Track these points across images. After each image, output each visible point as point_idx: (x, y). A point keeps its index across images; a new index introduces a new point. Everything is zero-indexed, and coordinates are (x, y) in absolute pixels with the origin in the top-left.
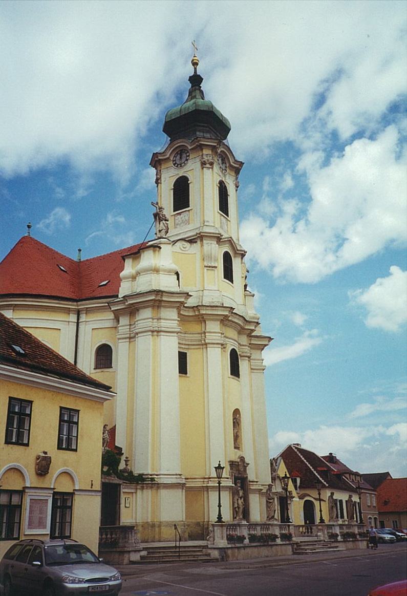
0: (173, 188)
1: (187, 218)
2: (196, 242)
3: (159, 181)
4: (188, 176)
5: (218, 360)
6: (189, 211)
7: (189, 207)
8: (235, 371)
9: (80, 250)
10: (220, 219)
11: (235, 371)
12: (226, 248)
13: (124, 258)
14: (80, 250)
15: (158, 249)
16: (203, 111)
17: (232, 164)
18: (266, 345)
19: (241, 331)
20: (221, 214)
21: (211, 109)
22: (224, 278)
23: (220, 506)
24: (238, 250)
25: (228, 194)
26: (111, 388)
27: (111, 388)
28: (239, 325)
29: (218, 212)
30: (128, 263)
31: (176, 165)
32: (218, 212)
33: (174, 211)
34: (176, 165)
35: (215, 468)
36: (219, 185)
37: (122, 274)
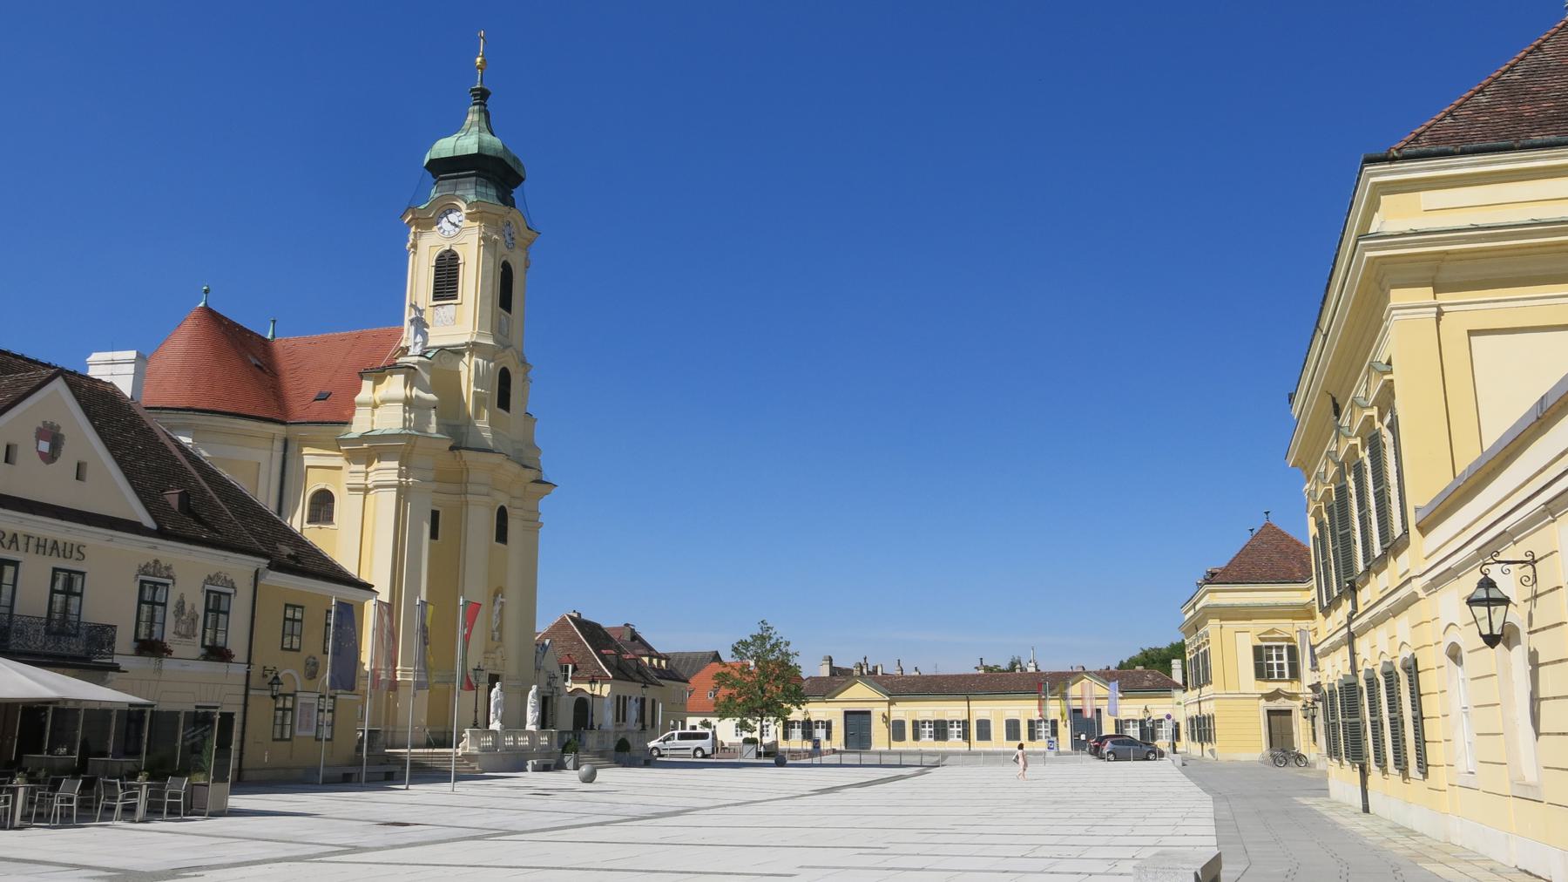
0: (434, 264)
1: (453, 314)
6: (456, 304)
7: (456, 298)
8: (502, 535)
10: (500, 319)
11: (502, 535)
13: (362, 376)
14: (274, 321)
16: (491, 156)
23: (476, 712)
26: (373, 586)
30: (367, 385)
31: (442, 231)
33: (434, 300)
34: (442, 231)
35: (474, 670)
37: (358, 398)
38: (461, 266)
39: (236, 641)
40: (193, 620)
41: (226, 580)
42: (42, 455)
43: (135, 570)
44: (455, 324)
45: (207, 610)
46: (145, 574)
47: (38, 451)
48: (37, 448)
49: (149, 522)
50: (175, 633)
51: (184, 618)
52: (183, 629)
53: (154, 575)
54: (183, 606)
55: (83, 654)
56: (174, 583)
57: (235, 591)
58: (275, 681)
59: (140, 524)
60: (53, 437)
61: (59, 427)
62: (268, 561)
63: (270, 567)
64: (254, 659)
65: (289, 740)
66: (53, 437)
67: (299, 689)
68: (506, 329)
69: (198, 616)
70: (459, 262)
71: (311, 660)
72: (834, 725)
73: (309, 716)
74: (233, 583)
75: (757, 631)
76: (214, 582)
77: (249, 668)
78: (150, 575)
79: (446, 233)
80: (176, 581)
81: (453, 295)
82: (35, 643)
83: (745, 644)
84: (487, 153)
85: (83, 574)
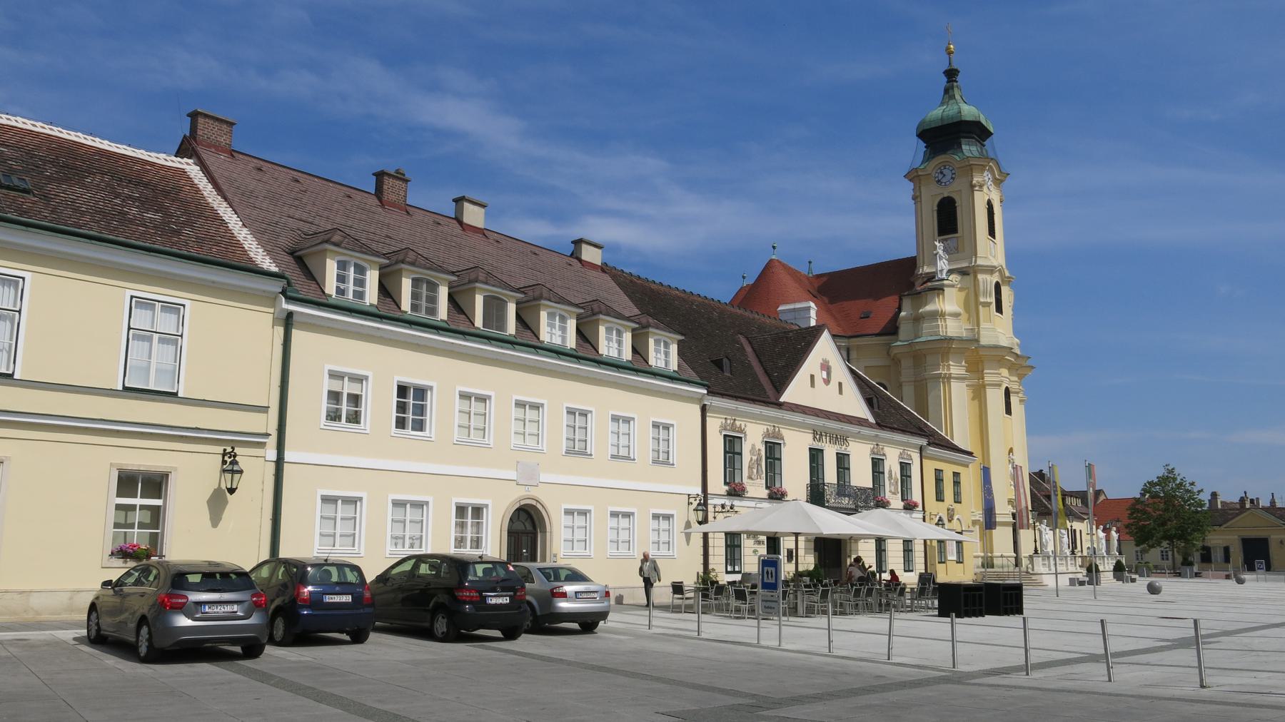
2: (968, 274)
3: (919, 199)
4: (954, 197)
5: (995, 398)
6: (957, 237)
9: (810, 262)
12: (996, 278)
14: (810, 262)
15: (941, 291)
18: (1026, 375)
19: (1012, 368)
21: (978, 120)
23: (1035, 541)
24: (1005, 277)
26: (973, 453)
28: (1011, 361)
39: (916, 496)
43: (869, 452)
44: (958, 252)
45: (902, 476)
46: (874, 453)
49: (872, 420)
51: (892, 481)
52: (893, 488)
55: (853, 507)
58: (940, 523)
60: (826, 367)
63: (929, 444)
64: (926, 509)
65: (944, 563)
66: (826, 367)
72: (1232, 550)
75: (1161, 472)
79: (943, 184)
81: (955, 231)
83: (1151, 484)
85: (849, 455)
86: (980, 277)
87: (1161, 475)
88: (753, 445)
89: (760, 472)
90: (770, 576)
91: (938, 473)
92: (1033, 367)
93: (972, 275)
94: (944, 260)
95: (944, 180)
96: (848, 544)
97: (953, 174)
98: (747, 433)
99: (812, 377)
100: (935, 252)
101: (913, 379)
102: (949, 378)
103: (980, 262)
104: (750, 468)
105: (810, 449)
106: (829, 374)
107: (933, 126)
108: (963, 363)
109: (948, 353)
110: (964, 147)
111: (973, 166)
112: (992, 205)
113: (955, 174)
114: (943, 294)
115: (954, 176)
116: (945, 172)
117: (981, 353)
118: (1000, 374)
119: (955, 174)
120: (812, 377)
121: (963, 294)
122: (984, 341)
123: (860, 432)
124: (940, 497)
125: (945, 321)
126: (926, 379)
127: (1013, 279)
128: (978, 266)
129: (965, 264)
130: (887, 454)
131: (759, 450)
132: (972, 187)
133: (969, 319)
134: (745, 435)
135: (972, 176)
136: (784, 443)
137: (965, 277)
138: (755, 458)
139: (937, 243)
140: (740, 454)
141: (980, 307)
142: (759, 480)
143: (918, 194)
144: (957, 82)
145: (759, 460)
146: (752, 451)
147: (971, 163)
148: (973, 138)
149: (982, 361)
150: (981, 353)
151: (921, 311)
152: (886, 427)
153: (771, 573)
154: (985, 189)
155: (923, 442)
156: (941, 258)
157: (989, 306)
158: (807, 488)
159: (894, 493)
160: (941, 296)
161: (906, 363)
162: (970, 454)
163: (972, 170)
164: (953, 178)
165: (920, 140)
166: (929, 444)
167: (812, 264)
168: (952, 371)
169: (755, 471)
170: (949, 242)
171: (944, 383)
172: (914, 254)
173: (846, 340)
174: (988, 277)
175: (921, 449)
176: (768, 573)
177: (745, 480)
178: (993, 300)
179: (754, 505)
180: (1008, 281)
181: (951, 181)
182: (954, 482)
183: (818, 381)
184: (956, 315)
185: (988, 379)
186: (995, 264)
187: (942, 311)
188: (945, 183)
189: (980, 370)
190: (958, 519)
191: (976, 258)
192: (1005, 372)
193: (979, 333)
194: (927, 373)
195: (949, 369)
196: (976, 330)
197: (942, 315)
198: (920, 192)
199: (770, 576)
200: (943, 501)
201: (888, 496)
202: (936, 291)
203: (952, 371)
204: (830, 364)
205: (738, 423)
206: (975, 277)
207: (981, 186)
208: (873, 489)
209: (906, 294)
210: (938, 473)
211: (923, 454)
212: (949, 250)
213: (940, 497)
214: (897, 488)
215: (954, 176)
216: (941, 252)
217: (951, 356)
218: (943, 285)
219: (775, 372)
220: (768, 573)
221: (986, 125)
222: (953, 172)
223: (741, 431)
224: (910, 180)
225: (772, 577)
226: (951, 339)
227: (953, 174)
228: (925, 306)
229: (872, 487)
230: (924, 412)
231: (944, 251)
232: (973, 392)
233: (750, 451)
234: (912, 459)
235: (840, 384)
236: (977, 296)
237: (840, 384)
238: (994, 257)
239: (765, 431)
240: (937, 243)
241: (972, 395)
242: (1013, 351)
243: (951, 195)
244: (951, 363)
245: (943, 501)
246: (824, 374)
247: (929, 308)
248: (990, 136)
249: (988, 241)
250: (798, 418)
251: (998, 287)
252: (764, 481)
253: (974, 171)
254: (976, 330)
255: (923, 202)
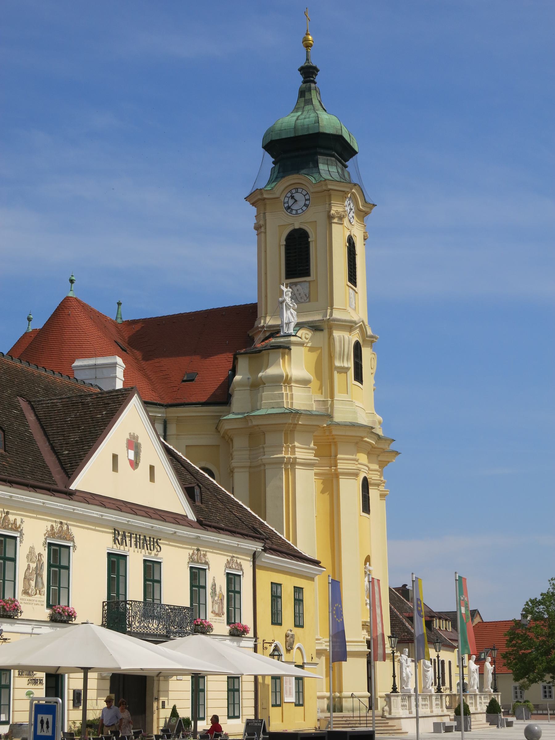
1: (307, 291)
2: (322, 330)
3: (263, 229)
6: (309, 282)
9: (119, 304)
12: (355, 337)
14: (119, 304)
15: (287, 350)
17: (361, 207)
18: (389, 462)
19: (372, 452)
20: (349, 287)
21: (339, 133)
22: (355, 380)
24: (367, 337)
25: (356, 253)
26: (320, 563)
27: (320, 563)
29: (347, 285)
32: (347, 285)
36: (348, 244)
38: (311, 244)
40: (221, 600)
41: (237, 563)
42: (131, 461)
43: (187, 560)
44: (309, 301)
45: (228, 591)
46: (193, 561)
47: (129, 459)
48: (128, 457)
49: (192, 517)
50: (212, 612)
51: (216, 598)
53: (198, 562)
54: (215, 588)
55: (164, 632)
56: (209, 568)
57: (243, 573)
58: (276, 653)
59: (186, 516)
61: (137, 437)
62: (263, 545)
63: (265, 550)
64: (259, 634)
65: (279, 706)
67: (305, 662)
68: (354, 302)
69: (223, 596)
70: (310, 240)
71: (289, 632)
73: (290, 684)
74: (241, 566)
76: (231, 565)
77: (256, 641)
78: (195, 562)
79: (294, 212)
80: (210, 566)
81: (307, 273)
82: (153, 625)
83: (534, 602)
84: (327, 131)
85: (160, 563)
86: (337, 334)
87: (545, 592)
88: (32, 549)
89: (40, 585)
90: (45, 726)
91: (275, 586)
92: (397, 453)
93: (326, 332)
94: (291, 310)
95: (294, 207)
96: (156, 683)
97: (306, 200)
98: (24, 532)
99: (115, 457)
100: (280, 299)
101: (248, 464)
102: (293, 464)
103: (337, 315)
104: (27, 579)
105: (109, 554)
106: (137, 455)
107: (284, 136)
108: (312, 445)
109: (292, 431)
110: (322, 167)
111: (332, 192)
112: (354, 243)
113: (309, 200)
114: (289, 354)
115: (307, 202)
116: (297, 196)
117: (334, 433)
118: (357, 461)
119: (309, 200)
120: (115, 457)
121: (314, 356)
122: (338, 417)
123: (175, 533)
124: (276, 620)
125: (291, 390)
126: (264, 465)
127: (376, 338)
128: (335, 320)
129: (317, 317)
130: (210, 563)
131: (40, 555)
132: (330, 218)
133: (321, 388)
134: (22, 535)
135: (330, 204)
136: (74, 546)
137: (318, 334)
138: (33, 565)
139: (283, 288)
140: (14, 560)
141: (336, 374)
142: (38, 596)
143: (262, 223)
144: (315, 83)
145: (38, 569)
146: (30, 556)
147: (330, 187)
148: (333, 156)
149: (335, 444)
150: (334, 433)
151: (260, 374)
152: (210, 526)
153: (47, 723)
154: (346, 221)
155: (258, 546)
156: (288, 308)
157: (346, 373)
158: (103, 607)
159: (218, 615)
160: (286, 356)
161: (240, 443)
162: (316, 563)
163: (330, 196)
164: (305, 205)
165: (267, 153)
166: (265, 550)
167: (121, 307)
168: (298, 455)
169: (33, 583)
170: (299, 287)
171: (287, 470)
172: (255, 301)
173: (163, 410)
174: (345, 335)
175: (254, 556)
176: (42, 721)
177: (19, 596)
178: (350, 364)
179: (30, 631)
180: (371, 341)
181: (304, 208)
182: (295, 599)
183: (123, 463)
184: (305, 382)
185: (342, 466)
186: (355, 318)
187: (287, 376)
188: (297, 210)
189: (333, 454)
190: (299, 648)
191: (332, 309)
192: (363, 458)
193: (332, 406)
194: (264, 457)
195: (293, 452)
196: (330, 402)
197: (287, 381)
198: (265, 220)
199: (45, 726)
200: (281, 624)
201: (210, 618)
202: (281, 350)
203: (298, 455)
204: (139, 441)
205: (11, 518)
206: (330, 334)
207: (341, 218)
208: (191, 609)
209: (242, 351)
210: (275, 586)
211: (257, 563)
212: (299, 299)
213: (276, 620)
214: (222, 608)
215: (307, 202)
216: (288, 300)
217: (296, 435)
218: (290, 343)
219: (66, 450)
220: (42, 721)
221: (349, 141)
222: (307, 197)
223: (16, 528)
224: (253, 204)
225: (48, 727)
226: (296, 414)
227: (306, 200)
228: (267, 367)
229: (189, 606)
230: (261, 509)
231: (292, 298)
232: (323, 483)
233: (27, 557)
234: (242, 570)
235: (152, 468)
236: (331, 358)
237: (152, 468)
238: (355, 309)
239: (49, 529)
240: (283, 288)
241: (321, 486)
242: (373, 430)
243: (303, 227)
244: (296, 444)
245: (281, 624)
246: (132, 454)
247: (271, 371)
248: (354, 155)
249: (347, 287)
250: (94, 512)
251: (357, 348)
252: (44, 598)
253: (332, 196)
254: (330, 402)
255: (267, 234)
